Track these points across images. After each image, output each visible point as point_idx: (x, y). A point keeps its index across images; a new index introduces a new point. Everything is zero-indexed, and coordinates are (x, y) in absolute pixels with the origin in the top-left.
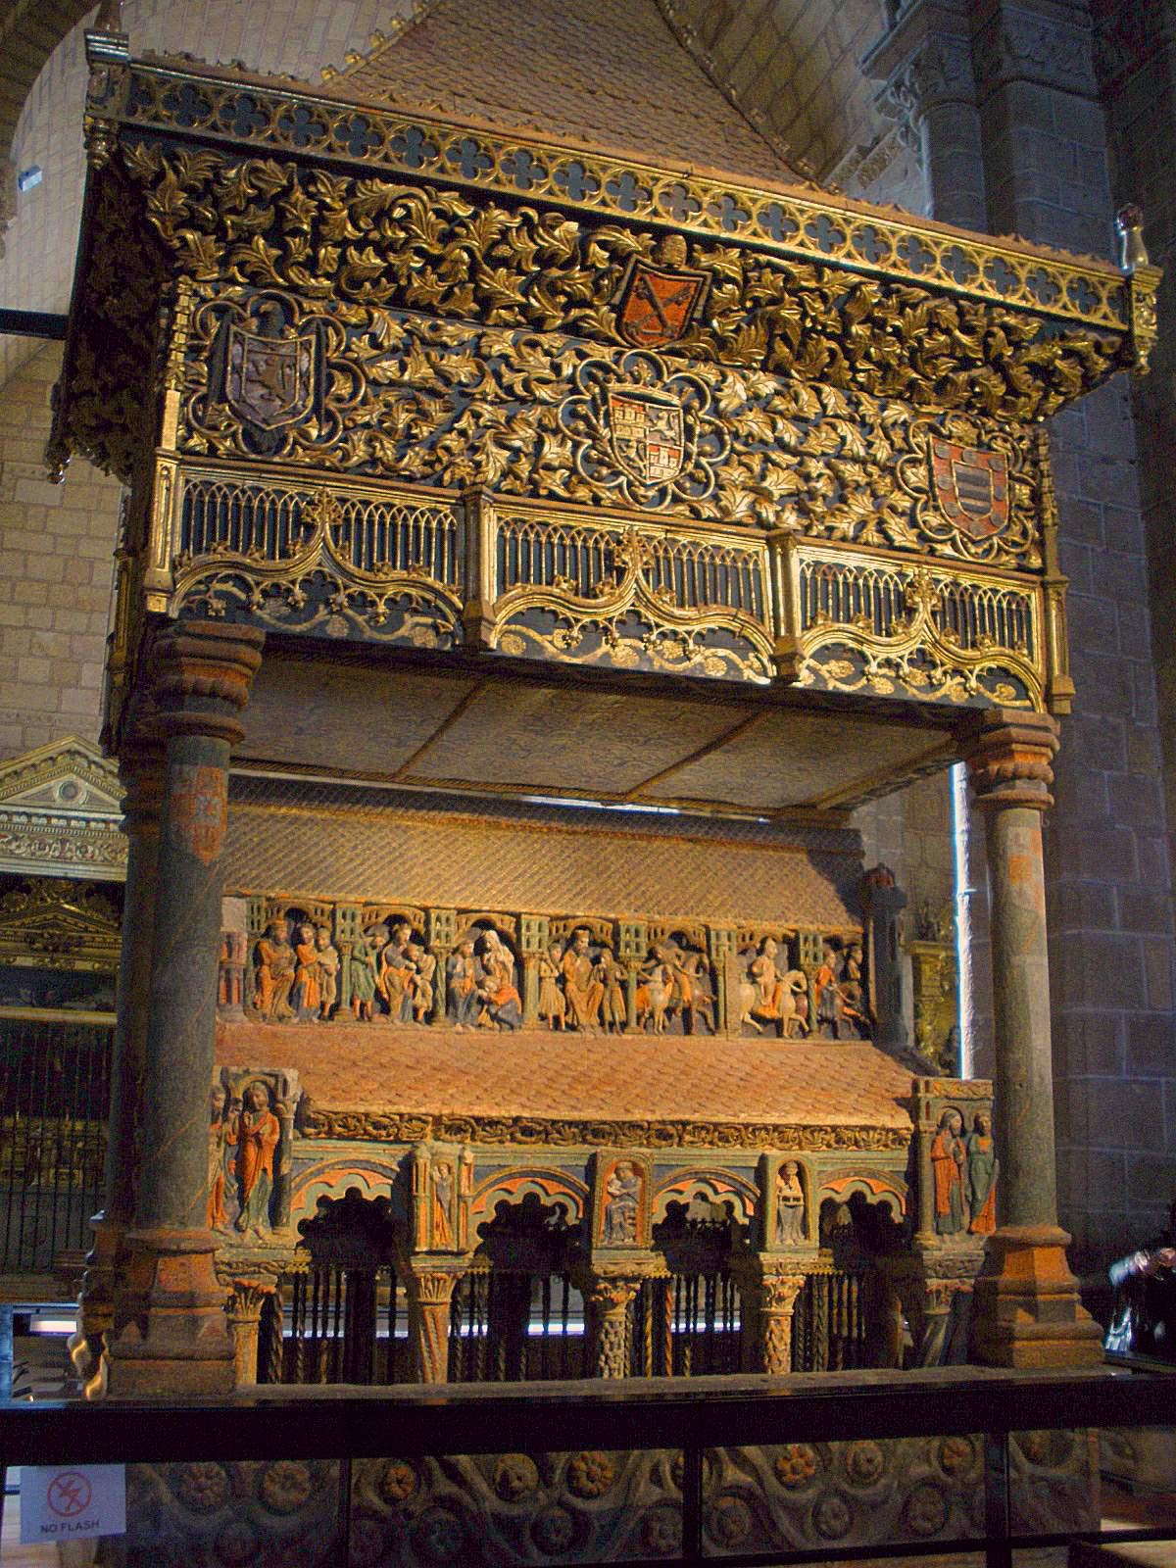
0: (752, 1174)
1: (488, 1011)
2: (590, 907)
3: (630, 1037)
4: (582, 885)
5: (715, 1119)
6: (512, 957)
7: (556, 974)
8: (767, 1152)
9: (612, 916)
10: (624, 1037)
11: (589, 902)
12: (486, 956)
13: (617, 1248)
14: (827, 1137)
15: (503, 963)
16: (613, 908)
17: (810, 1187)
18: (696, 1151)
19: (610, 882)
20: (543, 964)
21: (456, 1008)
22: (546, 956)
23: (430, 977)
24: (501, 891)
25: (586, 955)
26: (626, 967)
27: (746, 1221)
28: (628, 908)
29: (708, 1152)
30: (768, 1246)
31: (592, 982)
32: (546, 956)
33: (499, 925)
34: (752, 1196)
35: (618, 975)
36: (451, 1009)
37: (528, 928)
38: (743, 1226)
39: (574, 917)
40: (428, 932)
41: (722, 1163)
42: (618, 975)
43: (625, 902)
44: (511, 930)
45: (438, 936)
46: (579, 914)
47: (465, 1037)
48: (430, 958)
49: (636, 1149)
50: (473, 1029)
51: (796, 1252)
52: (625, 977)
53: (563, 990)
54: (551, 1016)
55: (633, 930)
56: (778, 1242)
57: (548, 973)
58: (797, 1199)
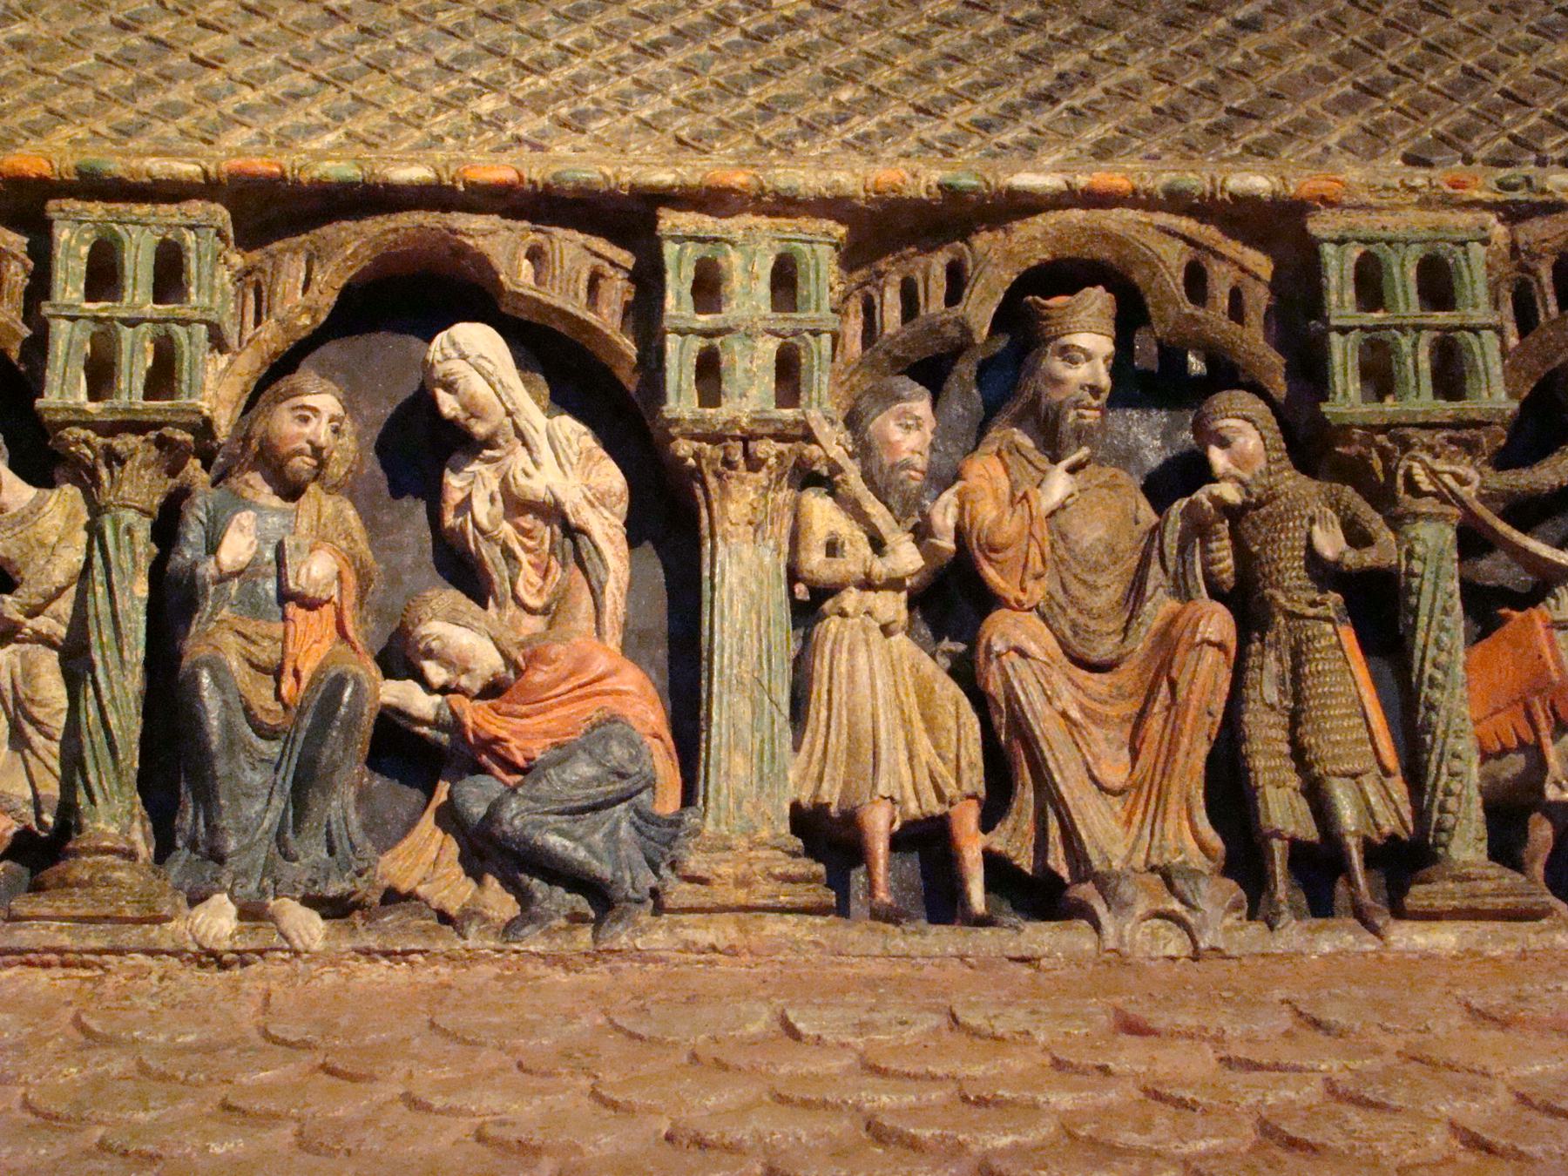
1: (450, 818)
2: (1102, 151)
3: (1445, 938)
4: (1066, 62)
6: (612, 477)
7: (906, 558)
9: (1257, 182)
10: (1408, 937)
11: (1094, 132)
12: (455, 483)
15: (552, 512)
16: (1263, 151)
19: (1250, 43)
20: (822, 513)
21: (206, 797)
22: (833, 443)
23: (54, 624)
24: (539, 103)
25: (1127, 457)
26: (1381, 497)
28: (1375, 139)
31: (1159, 606)
32: (833, 443)
33: (519, 277)
35: (1330, 542)
36: (188, 818)
37: (708, 288)
39: (1023, 205)
40: (38, 345)
42: (1330, 542)
43: (1344, 127)
44: (608, 318)
45: (101, 375)
46: (1027, 180)
47: (252, 979)
48: (64, 504)
50: (308, 927)
52: (1384, 551)
53: (965, 673)
54: (879, 824)
55: (1404, 275)
57: (857, 558)
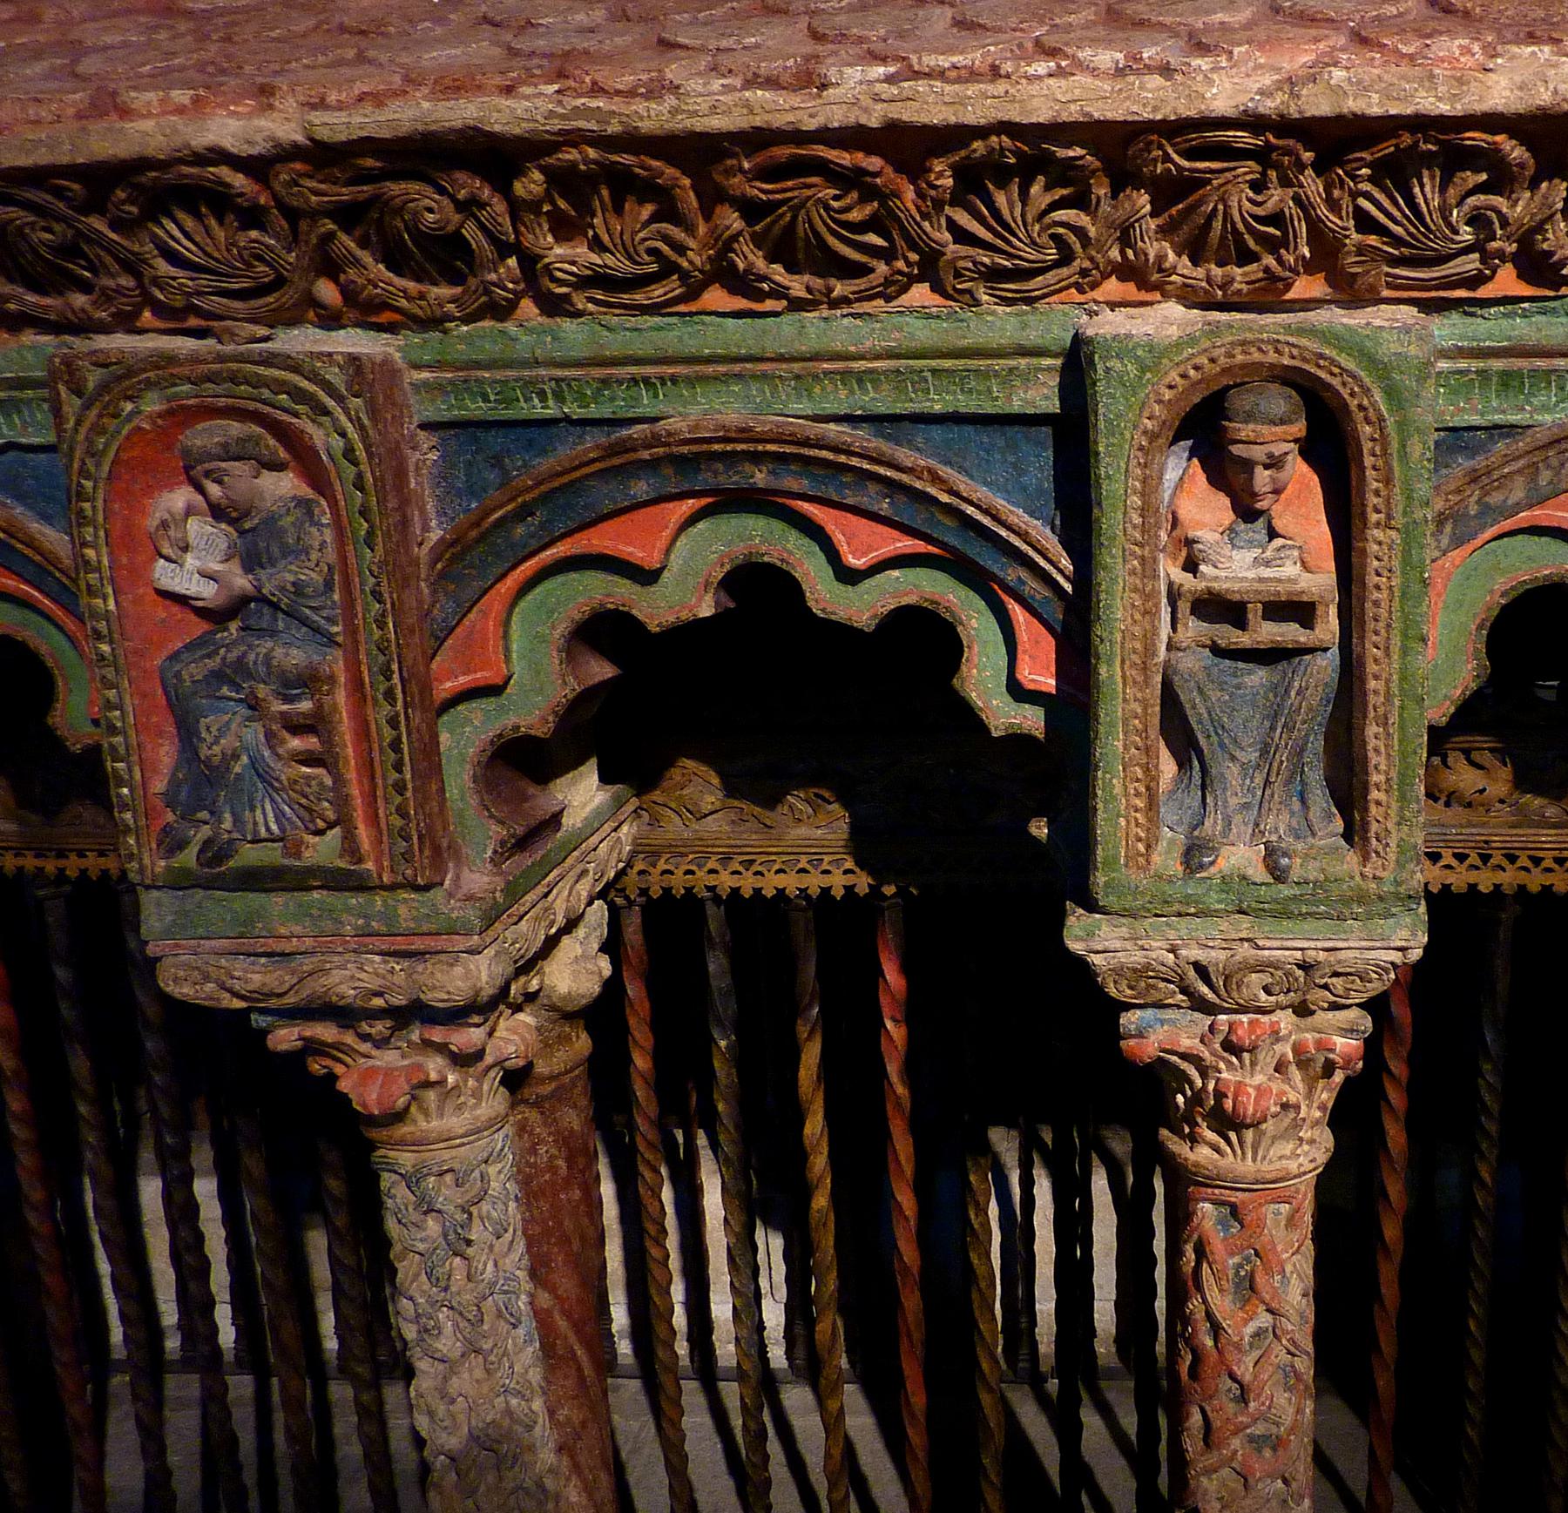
0: (1040, 465)
5: (653, 116)
8: (1108, 324)
13: (256, 880)
14: (1519, 208)
17: (1378, 541)
18: (672, 335)
27: (1031, 719)
29: (737, 335)
30: (1100, 878)
34: (1033, 586)
38: (1018, 741)
41: (841, 400)
49: (300, 340)
51: (1283, 912)
56: (1167, 860)
58: (1300, 611)
